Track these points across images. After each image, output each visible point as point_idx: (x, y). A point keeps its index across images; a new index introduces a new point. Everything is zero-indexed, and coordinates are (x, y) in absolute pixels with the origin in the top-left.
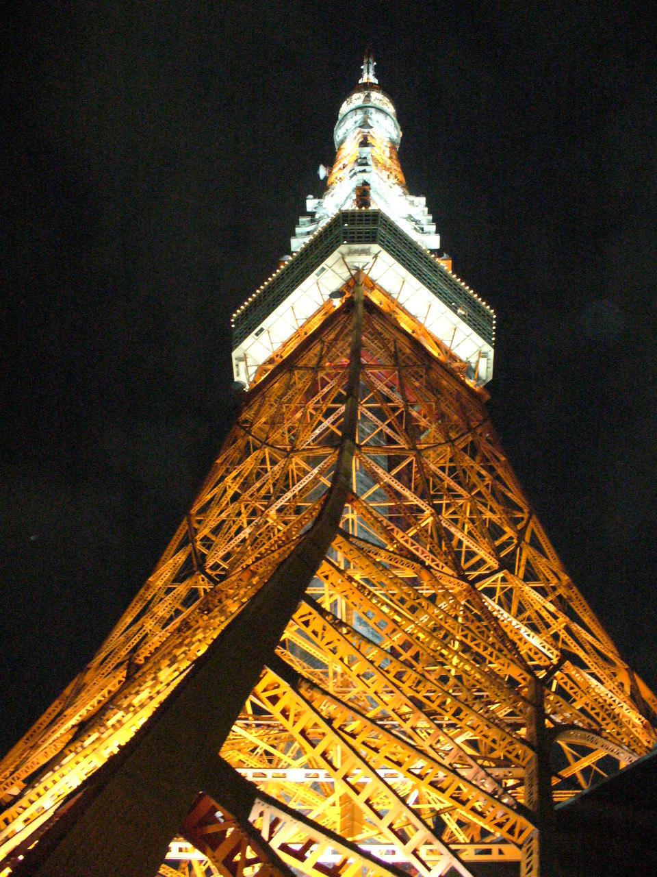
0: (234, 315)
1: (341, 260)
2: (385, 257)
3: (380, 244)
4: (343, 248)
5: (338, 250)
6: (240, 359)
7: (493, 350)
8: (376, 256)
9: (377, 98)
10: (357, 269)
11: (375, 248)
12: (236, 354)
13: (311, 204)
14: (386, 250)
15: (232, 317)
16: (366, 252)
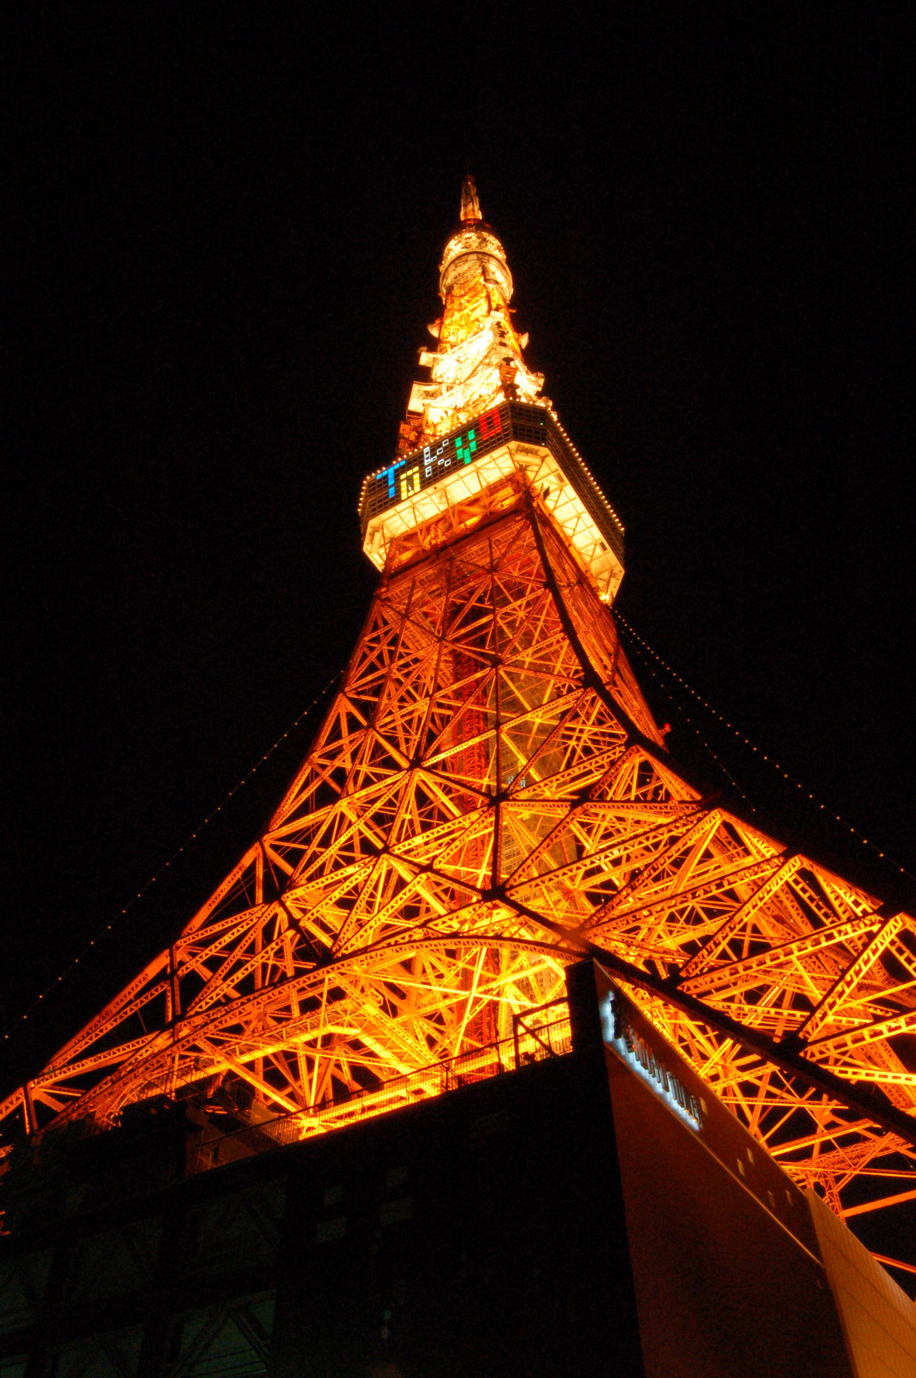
0: (368, 477)
1: (508, 456)
2: (552, 463)
3: (551, 450)
4: (513, 444)
5: (507, 445)
6: (376, 530)
7: (623, 572)
8: (543, 459)
9: (493, 245)
10: (521, 466)
11: (544, 451)
12: (373, 523)
13: (425, 358)
14: (555, 456)
15: (365, 479)
16: (535, 453)
